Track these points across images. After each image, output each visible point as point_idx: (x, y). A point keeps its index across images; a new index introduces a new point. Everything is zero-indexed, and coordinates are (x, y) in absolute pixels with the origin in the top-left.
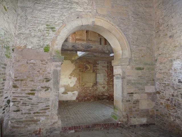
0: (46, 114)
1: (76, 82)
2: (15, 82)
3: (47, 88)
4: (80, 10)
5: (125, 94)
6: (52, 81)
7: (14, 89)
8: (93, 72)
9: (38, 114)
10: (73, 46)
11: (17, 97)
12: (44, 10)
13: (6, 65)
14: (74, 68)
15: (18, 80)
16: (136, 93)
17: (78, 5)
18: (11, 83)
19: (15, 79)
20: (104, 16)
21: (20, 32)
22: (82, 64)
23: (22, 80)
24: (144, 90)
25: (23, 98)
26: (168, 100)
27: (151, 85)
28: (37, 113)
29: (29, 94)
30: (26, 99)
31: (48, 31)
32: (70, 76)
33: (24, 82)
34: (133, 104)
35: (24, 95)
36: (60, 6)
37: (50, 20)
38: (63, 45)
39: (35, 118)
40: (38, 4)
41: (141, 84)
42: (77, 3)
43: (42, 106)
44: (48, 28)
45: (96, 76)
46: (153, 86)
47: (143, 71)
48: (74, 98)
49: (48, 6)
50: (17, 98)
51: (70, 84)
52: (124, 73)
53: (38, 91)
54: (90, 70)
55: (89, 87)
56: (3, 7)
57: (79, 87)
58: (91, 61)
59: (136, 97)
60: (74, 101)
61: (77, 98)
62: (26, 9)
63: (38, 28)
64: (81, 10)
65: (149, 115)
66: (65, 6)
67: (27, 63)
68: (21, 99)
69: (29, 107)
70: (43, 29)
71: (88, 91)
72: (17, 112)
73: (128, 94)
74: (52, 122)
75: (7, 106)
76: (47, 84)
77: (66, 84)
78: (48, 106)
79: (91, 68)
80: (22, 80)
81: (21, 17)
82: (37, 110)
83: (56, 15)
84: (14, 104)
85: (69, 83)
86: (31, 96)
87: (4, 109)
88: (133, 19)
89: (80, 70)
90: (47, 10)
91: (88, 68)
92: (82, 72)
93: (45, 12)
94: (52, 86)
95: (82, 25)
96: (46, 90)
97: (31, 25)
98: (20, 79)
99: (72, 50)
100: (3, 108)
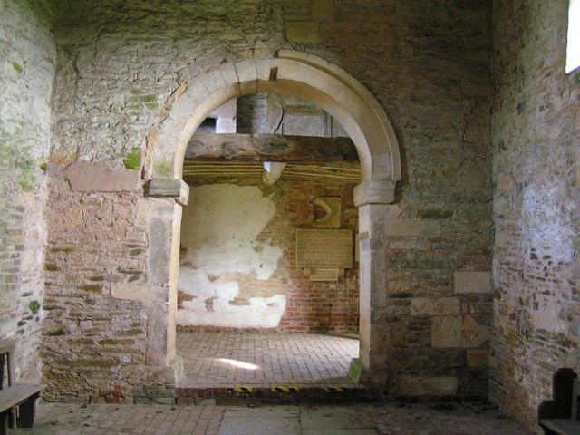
0: (133, 347)
1: (280, 262)
2: (52, 256)
3: (135, 275)
4: (230, 38)
5: (382, 297)
6: (148, 252)
7: (50, 274)
8: (343, 227)
9: (113, 347)
10: (223, 146)
11: (58, 295)
12: (126, 49)
13: (22, 209)
14: (273, 212)
15: (57, 250)
16: (420, 295)
17: (225, 24)
18: (41, 258)
19: (51, 246)
20: (306, 47)
21: (62, 116)
22: (303, 197)
23: (67, 251)
24: (452, 285)
25: (74, 300)
26: (512, 317)
27: (476, 270)
28: (110, 342)
29: (87, 288)
30: (81, 301)
31: (137, 107)
32: (256, 244)
33: (74, 255)
34: (410, 329)
35: (73, 290)
36: (171, 33)
37: (142, 77)
38: (191, 144)
39: (106, 356)
40: (108, 35)
41: (440, 265)
42: (223, 18)
43: (121, 322)
44: (134, 100)
45: (354, 240)
46: (484, 273)
47: (446, 221)
48: (273, 321)
49: (138, 36)
50: (56, 298)
51: (259, 271)
52: (378, 227)
53: (109, 280)
54: (329, 219)
55: (326, 282)
56: (11, 67)
57: (290, 282)
58: (337, 188)
59: (418, 306)
60: (273, 331)
61: (283, 322)
62: (79, 53)
63: (110, 102)
64: (236, 37)
65: (467, 370)
66: (187, 29)
67: (81, 201)
68: (67, 303)
69: (88, 325)
70: (123, 103)
71: (324, 296)
72: (58, 337)
73: (393, 296)
74: (148, 370)
75: (30, 318)
76: (134, 264)
77: (244, 270)
78: (139, 324)
79: (334, 213)
80: (67, 251)
81: (66, 74)
82: (110, 335)
83: (160, 60)
84: (49, 314)
85: (256, 266)
86: (92, 295)
87: (20, 324)
88: (411, 51)
89: (293, 220)
90: (133, 48)
91: (325, 213)
92: (301, 226)
93: (130, 53)
94: (148, 270)
95: (239, 83)
96: (131, 280)
97: (91, 93)
98: (65, 246)
99: (222, 158)
100: (19, 319)
